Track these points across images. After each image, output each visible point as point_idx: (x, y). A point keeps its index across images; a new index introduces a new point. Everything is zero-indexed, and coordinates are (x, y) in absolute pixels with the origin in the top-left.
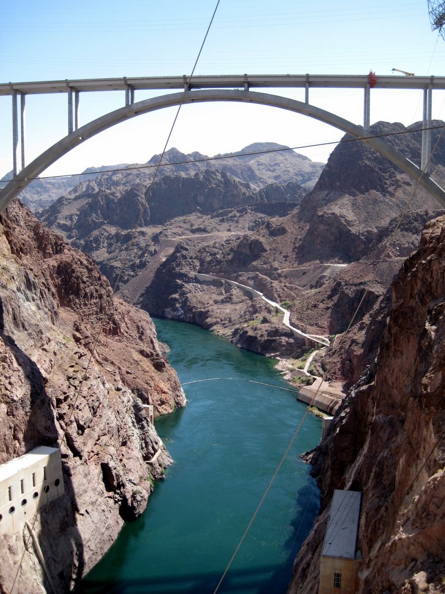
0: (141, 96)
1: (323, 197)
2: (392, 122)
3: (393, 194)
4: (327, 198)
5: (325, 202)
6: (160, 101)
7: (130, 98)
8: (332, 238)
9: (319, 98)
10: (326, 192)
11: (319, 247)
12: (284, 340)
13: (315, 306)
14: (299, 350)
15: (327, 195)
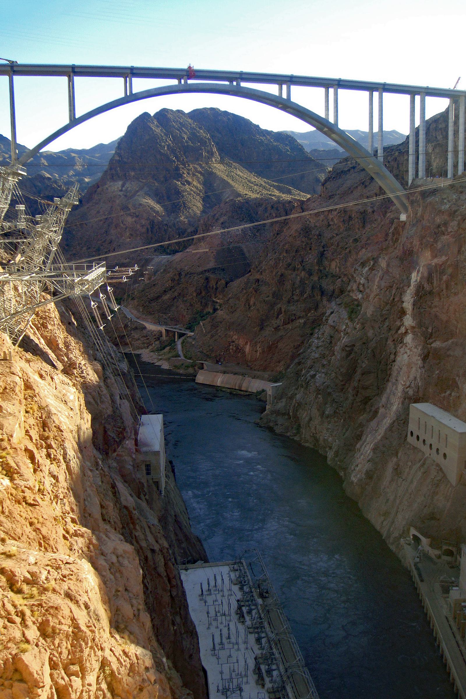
0: (140, 85)
1: (118, 188)
2: (174, 109)
3: (192, 183)
4: (124, 189)
5: (122, 193)
6: (270, 97)
7: (128, 86)
8: (144, 230)
9: (301, 96)
10: (120, 183)
11: (129, 240)
12: (136, 335)
13: (159, 297)
14: (157, 342)
15: (123, 186)
